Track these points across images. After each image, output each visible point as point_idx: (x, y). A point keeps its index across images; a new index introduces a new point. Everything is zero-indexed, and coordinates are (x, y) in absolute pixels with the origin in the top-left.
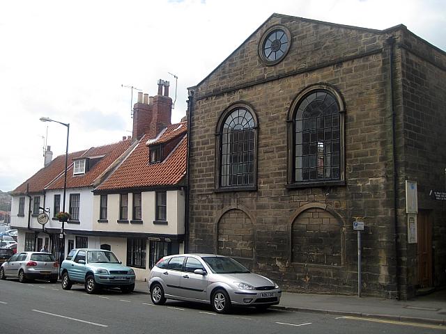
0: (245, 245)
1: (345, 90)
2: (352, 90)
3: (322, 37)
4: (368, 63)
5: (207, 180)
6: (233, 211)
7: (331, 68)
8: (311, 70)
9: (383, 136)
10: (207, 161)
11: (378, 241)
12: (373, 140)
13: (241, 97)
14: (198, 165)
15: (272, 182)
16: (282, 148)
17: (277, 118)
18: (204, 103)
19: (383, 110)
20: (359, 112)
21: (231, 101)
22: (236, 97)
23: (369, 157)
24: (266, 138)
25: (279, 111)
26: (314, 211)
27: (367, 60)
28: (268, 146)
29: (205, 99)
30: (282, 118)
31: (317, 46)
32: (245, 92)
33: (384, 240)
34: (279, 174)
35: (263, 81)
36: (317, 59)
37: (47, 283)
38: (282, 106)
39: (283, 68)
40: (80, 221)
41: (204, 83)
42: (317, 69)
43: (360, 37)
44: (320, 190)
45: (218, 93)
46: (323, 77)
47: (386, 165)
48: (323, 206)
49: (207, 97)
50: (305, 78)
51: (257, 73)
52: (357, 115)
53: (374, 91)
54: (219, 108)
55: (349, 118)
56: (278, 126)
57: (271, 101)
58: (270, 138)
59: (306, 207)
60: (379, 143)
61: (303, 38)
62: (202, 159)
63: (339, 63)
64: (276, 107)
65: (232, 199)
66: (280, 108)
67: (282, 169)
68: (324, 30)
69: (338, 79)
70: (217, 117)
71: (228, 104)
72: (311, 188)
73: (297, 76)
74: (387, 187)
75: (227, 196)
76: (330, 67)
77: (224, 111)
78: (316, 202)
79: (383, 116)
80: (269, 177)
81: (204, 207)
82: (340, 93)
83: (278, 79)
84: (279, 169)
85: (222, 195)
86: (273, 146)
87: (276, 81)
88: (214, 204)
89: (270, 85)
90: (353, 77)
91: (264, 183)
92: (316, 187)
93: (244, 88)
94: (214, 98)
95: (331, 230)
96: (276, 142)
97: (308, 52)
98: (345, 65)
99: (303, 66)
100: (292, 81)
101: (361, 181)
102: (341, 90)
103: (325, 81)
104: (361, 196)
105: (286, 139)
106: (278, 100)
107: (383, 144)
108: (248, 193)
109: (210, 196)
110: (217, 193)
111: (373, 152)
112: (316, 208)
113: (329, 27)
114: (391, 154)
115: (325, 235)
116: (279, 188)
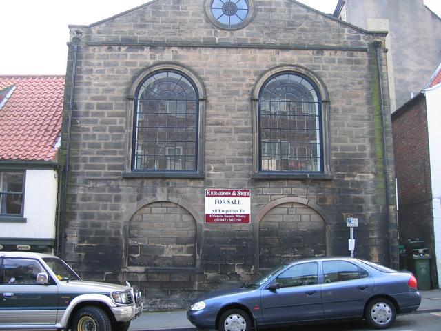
0: (181, 250)
1: (328, 79)
2: (336, 81)
3: (296, 17)
4: (353, 58)
5: (107, 160)
6: (159, 205)
7: (310, 52)
8: (284, 48)
9: (371, 133)
10: (107, 132)
11: (370, 239)
12: (361, 135)
13: (175, 57)
14: (87, 137)
15: (229, 169)
16: (244, 130)
17: (237, 93)
18: (103, 51)
19: (370, 108)
20: (344, 104)
21: (158, 59)
22: (167, 55)
23: (358, 152)
24: (219, 115)
25: (238, 85)
26: (290, 206)
27: (352, 55)
28: (221, 124)
29: (106, 47)
30: (244, 94)
31: (290, 26)
32: (181, 52)
33: (375, 237)
34: (241, 161)
35: (210, 45)
36: (291, 38)
37: (171, 310)
38: (243, 80)
39: (243, 35)
40: (68, 30)
41: (103, 25)
42: (292, 49)
43: (343, 31)
44: (300, 182)
45: (133, 44)
46: (300, 60)
47: (375, 162)
48: (304, 201)
49: (110, 45)
50: (276, 56)
51: (203, 33)
52: (342, 108)
53: (360, 86)
54: (134, 64)
55: (333, 109)
56: (237, 103)
57: (225, 71)
58: (225, 116)
59: (280, 201)
60: (367, 140)
61: (271, 10)
62: (96, 129)
63: (320, 49)
64: (233, 80)
65: (159, 189)
66: (241, 83)
67: (246, 154)
68: (299, 11)
69: (319, 66)
70: (129, 75)
71: (151, 62)
72: (288, 179)
73: (265, 51)
74: (375, 182)
75: (148, 184)
76: (308, 52)
77: (144, 70)
78: (294, 196)
79: (371, 113)
80: (223, 163)
81: (99, 199)
82: (321, 81)
83: (237, 48)
84: (240, 154)
85: (139, 182)
86: (229, 126)
87: (234, 50)
88: (121, 193)
89: (224, 51)
90: (336, 68)
91: (216, 170)
92: (298, 179)
93: (181, 47)
94: (123, 49)
95: (313, 228)
96: (234, 121)
97: (279, 28)
98: (326, 53)
99: (273, 41)
100: (260, 54)
101: (349, 176)
102: (324, 79)
103: (303, 65)
104: (350, 191)
105: (249, 120)
106: (238, 73)
107: (372, 141)
108: (188, 181)
109: (113, 183)
110: (127, 178)
111: (362, 148)
112: (292, 203)
113: (304, 10)
114: (379, 149)
115: (304, 234)
116: (240, 177)
